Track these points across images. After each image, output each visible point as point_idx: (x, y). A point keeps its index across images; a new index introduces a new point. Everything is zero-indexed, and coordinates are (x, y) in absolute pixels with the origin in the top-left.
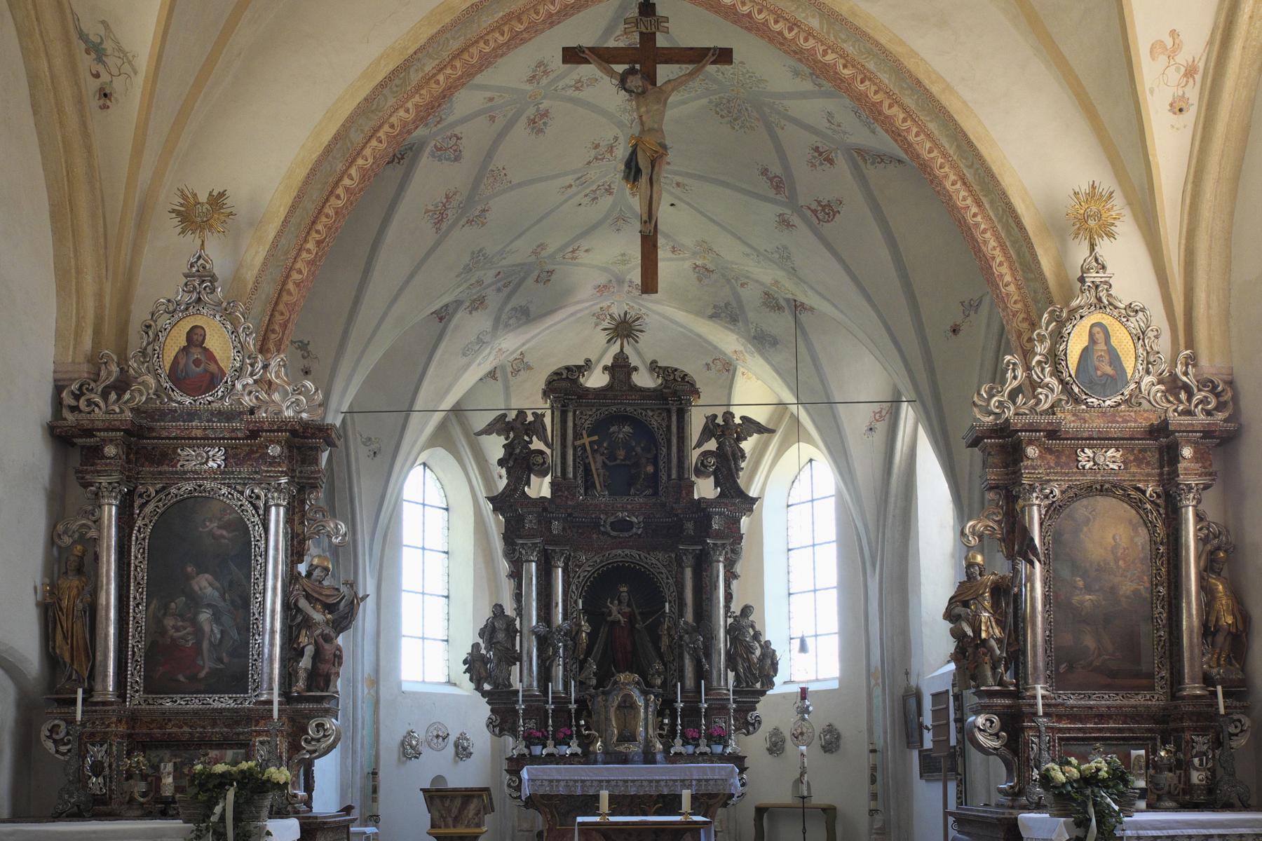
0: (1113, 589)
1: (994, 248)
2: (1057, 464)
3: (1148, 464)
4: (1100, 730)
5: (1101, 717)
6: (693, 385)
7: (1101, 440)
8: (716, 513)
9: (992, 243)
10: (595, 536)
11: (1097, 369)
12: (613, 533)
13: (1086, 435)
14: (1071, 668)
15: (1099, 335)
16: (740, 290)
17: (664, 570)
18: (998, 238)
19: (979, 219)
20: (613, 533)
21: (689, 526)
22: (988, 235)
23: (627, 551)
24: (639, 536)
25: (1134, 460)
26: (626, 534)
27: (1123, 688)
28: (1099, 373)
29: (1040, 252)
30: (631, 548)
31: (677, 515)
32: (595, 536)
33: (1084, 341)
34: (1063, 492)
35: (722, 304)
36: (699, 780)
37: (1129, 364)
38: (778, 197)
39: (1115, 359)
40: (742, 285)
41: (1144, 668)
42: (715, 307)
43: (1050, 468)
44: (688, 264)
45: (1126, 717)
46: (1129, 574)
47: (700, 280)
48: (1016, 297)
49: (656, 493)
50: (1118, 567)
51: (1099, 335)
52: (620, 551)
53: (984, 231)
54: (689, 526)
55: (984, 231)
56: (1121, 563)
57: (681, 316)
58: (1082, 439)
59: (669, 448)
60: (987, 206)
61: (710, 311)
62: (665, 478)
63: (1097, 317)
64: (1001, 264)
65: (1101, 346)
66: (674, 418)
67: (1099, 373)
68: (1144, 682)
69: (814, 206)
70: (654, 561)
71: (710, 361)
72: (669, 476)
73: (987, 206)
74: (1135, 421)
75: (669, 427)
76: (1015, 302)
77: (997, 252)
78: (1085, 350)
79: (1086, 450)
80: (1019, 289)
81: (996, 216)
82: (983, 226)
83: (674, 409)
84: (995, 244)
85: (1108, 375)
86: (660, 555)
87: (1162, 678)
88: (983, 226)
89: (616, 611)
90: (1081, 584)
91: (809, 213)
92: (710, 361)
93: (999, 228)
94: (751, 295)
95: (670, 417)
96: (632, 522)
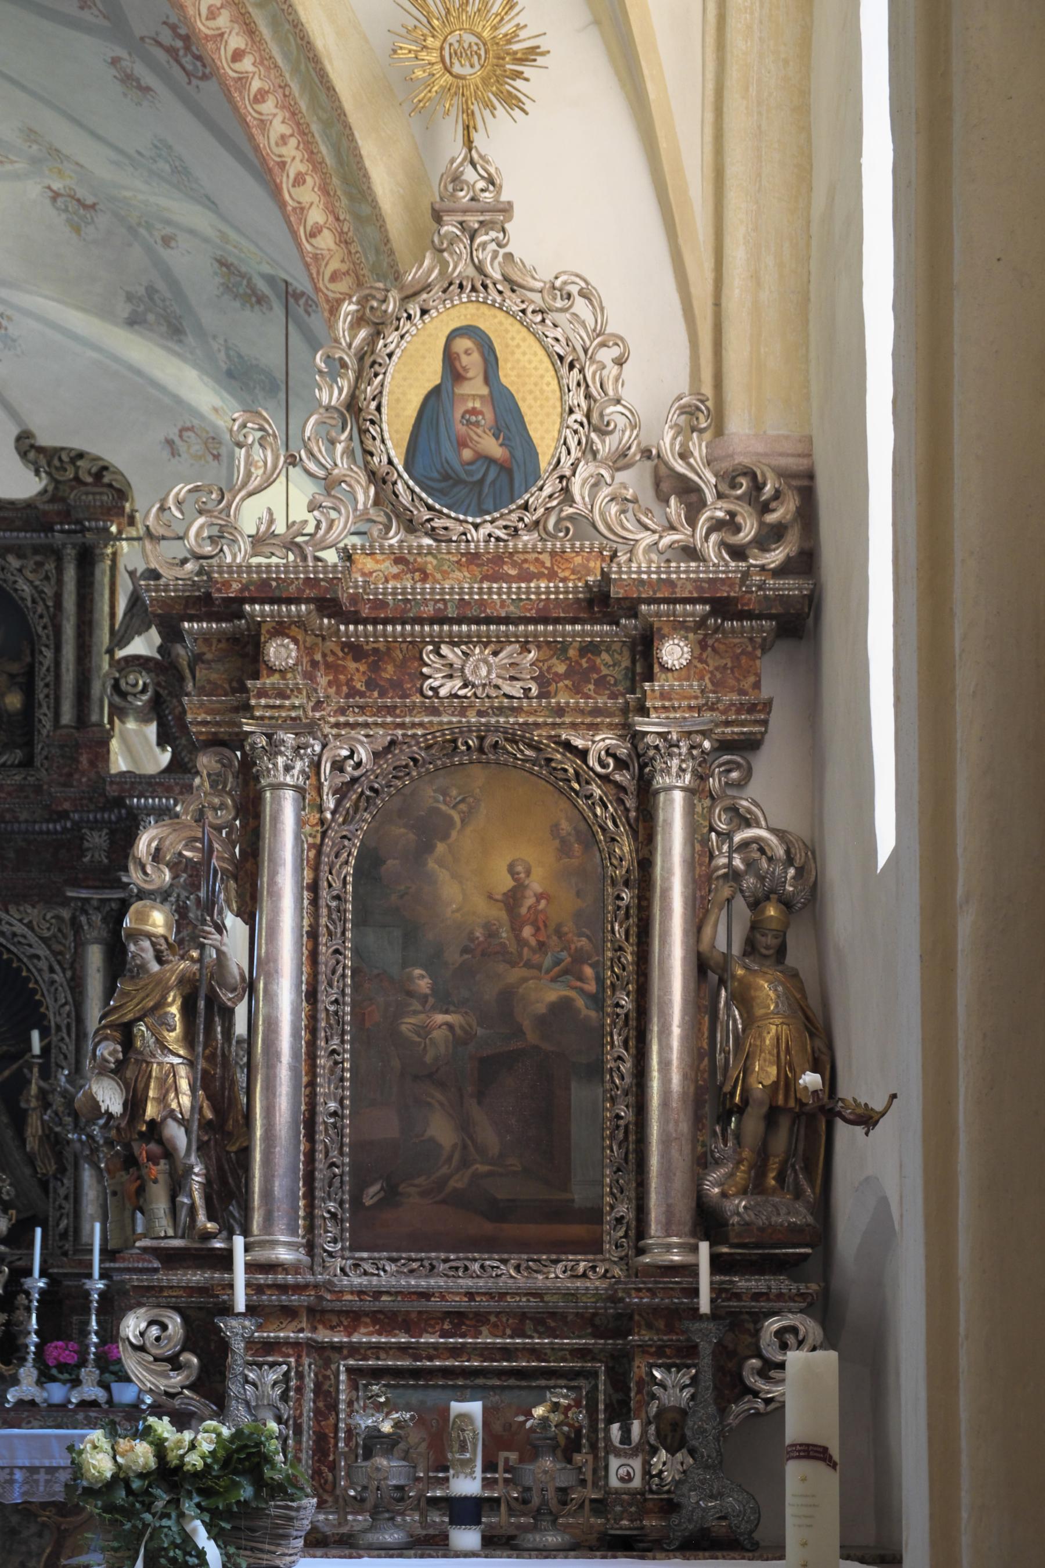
0: (508, 997)
1: (283, 139)
2: (370, 684)
3: (601, 683)
4: (455, 1351)
5: (458, 1320)
6: (122, 494)
7: (473, 620)
8: (150, 811)
9: (279, 127)
11: (462, 443)
13: (428, 611)
14: (391, 1196)
15: (468, 357)
16: (164, 253)
18: (294, 114)
19: (247, 64)
21: (97, 840)
22: (268, 107)
25: (567, 675)
27: (522, 1246)
28: (467, 454)
29: (368, 148)
31: (64, 815)
33: (432, 373)
34: (376, 755)
35: (141, 291)
36: (33, 1470)
37: (545, 430)
38: (87, 15)
39: (509, 419)
40: (167, 241)
41: (579, 1195)
42: (130, 297)
43: (353, 693)
44: (33, 189)
45: (523, 1321)
46: (548, 961)
47: (77, 230)
48: (335, 265)
49: (28, 763)
50: (521, 942)
51: (468, 357)
53: (260, 97)
54: (97, 840)
55: (260, 97)
56: (527, 932)
57: (78, 321)
58: (420, 621)
59: (58, 649)
60: (265, 31)
61: (124, 310)
62: (48, 724)
63: (462, 312)
64: (299, 180)
65: (475, 387)
66: (70, 574)
67: (467, 454)
68: (577, 1230)
69: (166, 37)
70: (19, 928)
71: (173, 434)
72: (57, 715)
73: (265, 31)
74: (552, 576)
75: (58, 597)
76: (334, 277)
77: (290, 150)
78: (435, 393)
79: (445, 650)
80: (344, 241)
81: (286, 55)
82: (256, 85)
83: (70, 552)
84: (285, 129)
85: (490, 460)
86: (33, 913)
87: (619, 1220)
88: (256, 85)
90: (424, 985)
91: (161, 56)
92: (173, 434)
93: (295, 88)
94: (192, 266)
95: (60, 570)
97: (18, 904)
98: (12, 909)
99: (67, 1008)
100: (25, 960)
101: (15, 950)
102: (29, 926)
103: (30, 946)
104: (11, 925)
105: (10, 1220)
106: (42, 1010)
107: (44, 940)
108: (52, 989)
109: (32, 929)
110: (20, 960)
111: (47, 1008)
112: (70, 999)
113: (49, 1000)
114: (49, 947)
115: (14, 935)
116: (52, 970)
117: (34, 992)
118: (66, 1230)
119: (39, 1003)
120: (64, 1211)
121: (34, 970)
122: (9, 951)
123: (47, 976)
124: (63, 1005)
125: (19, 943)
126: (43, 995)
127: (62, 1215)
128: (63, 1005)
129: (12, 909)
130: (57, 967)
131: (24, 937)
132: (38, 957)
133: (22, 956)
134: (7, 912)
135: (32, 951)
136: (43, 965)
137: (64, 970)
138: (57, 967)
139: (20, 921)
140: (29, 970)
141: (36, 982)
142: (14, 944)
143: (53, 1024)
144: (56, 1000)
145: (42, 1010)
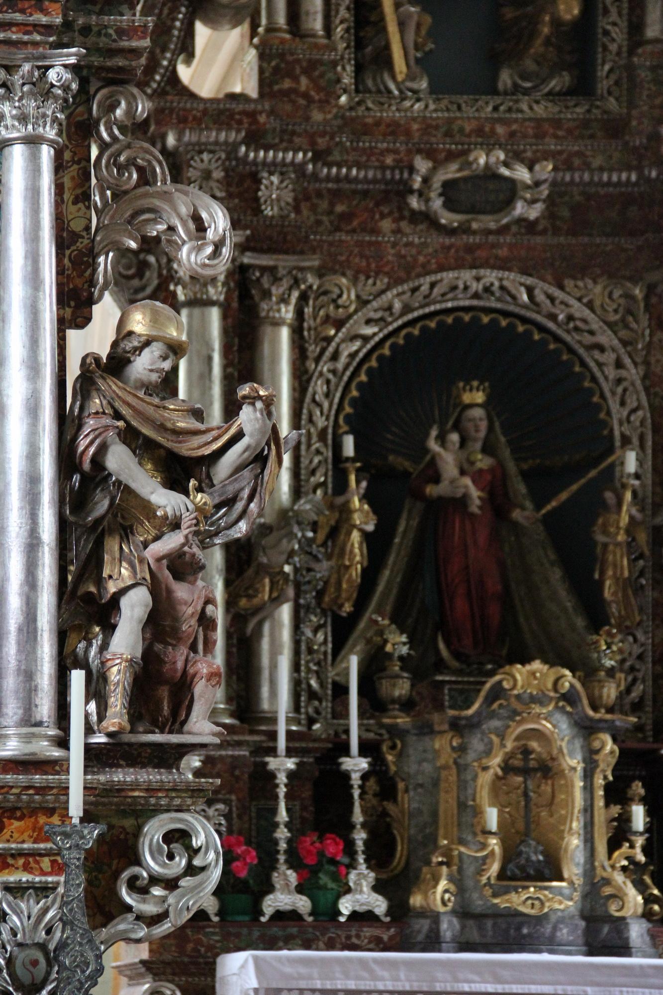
10: (386, 225)
12: (446, 218)
17: (606, 338)
20: (446, 218)
23: (491, 277)
24: (528, 226)
26: (490, 222)
30: (503, 265)
32: (386, 225)
52: (467, 275)
70: (578, 309)
89: (454, 466)
96: (511, 189)
97: (574, 278)
98: (569, 283)
99: (640, 413)
100: (581, 351)
101: (567, 338)
102: (590, 306)
103: (592, 333)
104: (567, 305)
105: (618, 686)
106: (602, 415)
107: (610, 325)
108: (620, 390)
109: (593, 310)
110: (571, 350)
111: (609, 413)
112: (645, 403)
113: (614, 404)
114: (615, 333)
115: (570, 318)
116: (619, 365)
117: (590, 392)
118: (642, 698)
119: (598, 408)
120: (640, 675)
121: (592, 364)
122: (557, 339)
123: (611, 373)
124: (634, 411)
125: (576, 329)
126: (602, 396)
127: (635, 680)
128: (634, 411)
129: (569, 283)
130: (627, 361)
131: (585, 321)
132: (601, 349)
133: (576, 347)
134: (561, 287)
135: (588, 339)
136: (609, 358)
137: (635, 364)
138: (627, 361)
139: (579, 299)
140: (583, 364)
141: (594, 379)
142: (568, 332)
143: (617, 433)
144: (623, 403)
145: (602, 415)
